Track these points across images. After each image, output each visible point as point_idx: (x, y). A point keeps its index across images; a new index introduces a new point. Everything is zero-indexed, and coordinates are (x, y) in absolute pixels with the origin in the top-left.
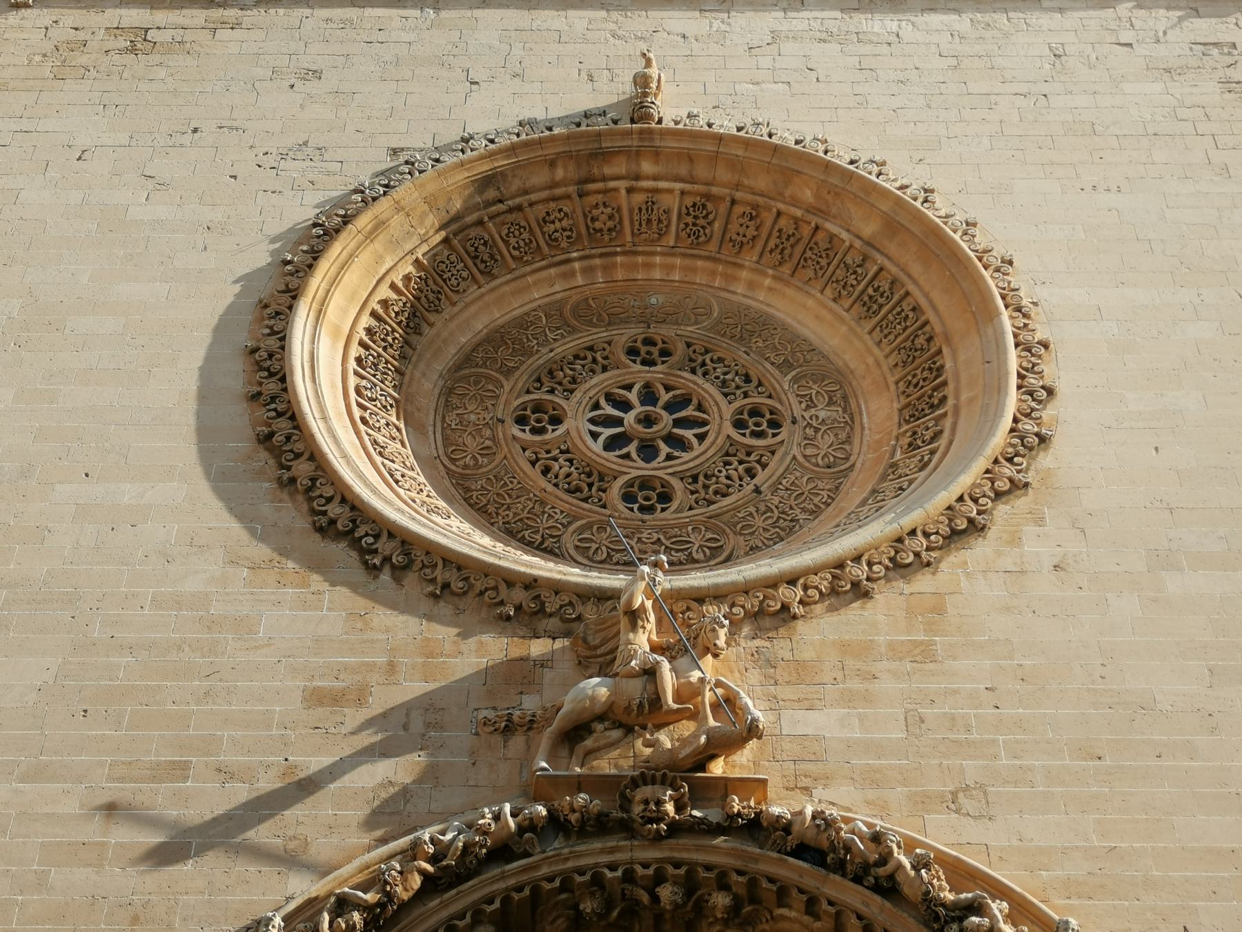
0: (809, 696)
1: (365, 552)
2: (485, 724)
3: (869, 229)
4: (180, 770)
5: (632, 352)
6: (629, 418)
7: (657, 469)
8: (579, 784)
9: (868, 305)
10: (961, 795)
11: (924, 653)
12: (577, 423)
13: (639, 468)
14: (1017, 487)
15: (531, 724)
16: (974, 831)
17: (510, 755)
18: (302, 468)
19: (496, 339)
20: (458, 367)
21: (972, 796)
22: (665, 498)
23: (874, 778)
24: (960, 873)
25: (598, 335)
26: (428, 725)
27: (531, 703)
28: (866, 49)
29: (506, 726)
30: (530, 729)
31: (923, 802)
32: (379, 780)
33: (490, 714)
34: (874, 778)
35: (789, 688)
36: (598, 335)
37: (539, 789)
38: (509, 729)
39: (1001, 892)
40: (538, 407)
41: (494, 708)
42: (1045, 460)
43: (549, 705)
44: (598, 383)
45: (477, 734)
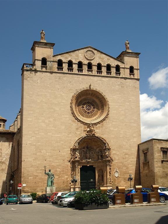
1: (78, 121)
3: (101, 97)
4: (71, 133)
5: (87, 103)
6: (87, 107)
7: (89, 111)
8: (88, 135)
9: (100, 101)
11: (102, 127)
12: (85, 108)
13: (88, 111)
14: (107, 117)
16: (104, 136)
18: (74, 115)
19: (80, 101)
20: (79, 103)
22: (89, 113)
23: (99, 133)
24: (103, 139)
25: (86, 101)
28: (102, 82)
31: (101, 135)
34: (99, 133)
36: (86, 101)
37: (86, 135)
38: (85, 131)
39: (104, 139)
40: (83, 107)
42: (108, 115)
44: (85, 106)
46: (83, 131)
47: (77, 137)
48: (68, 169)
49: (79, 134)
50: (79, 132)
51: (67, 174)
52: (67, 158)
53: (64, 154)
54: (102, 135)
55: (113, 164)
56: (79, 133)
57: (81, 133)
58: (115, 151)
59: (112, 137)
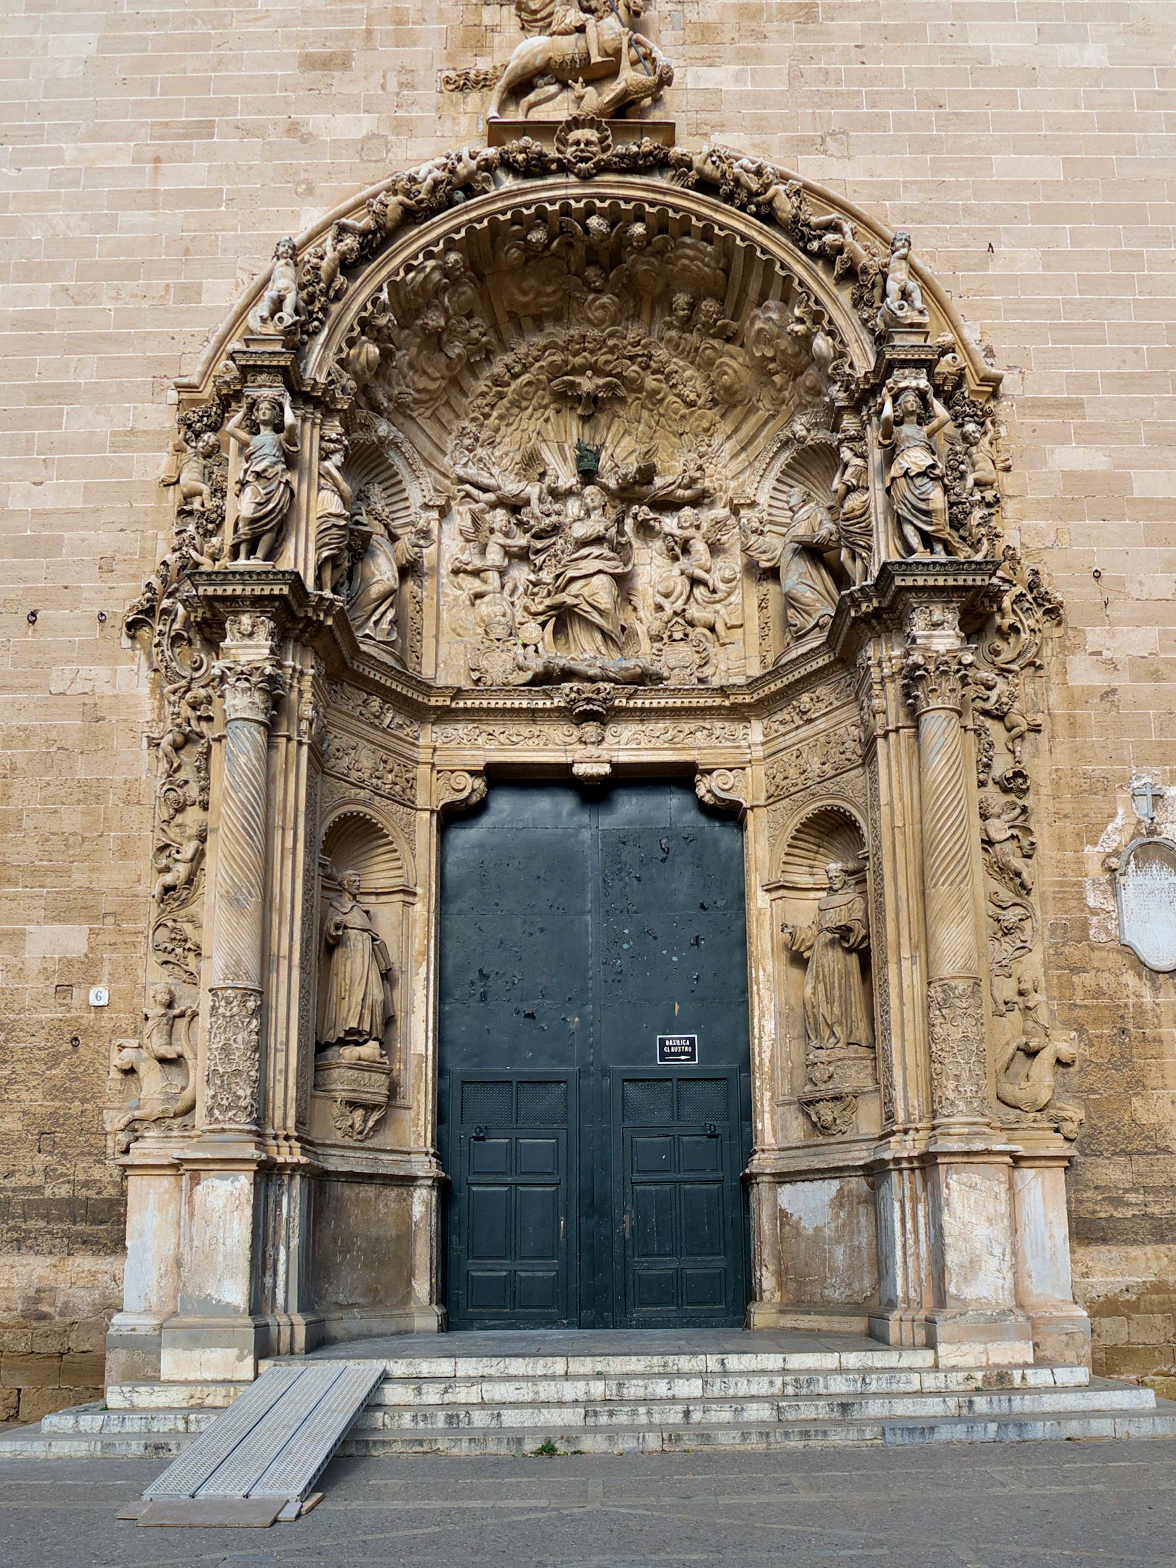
0: (711, 54)
2: (448, 82)
10: (828, 138)
15: (483, 83)
17: (469, 110)
21: (836, 140)
26: (401, 85)
27: (483, 65)
29: (465, 84)
30: (484, 86)
32: (364, 132)
33: (452, 74)
34: (759, 126)
35: (694, 47)
38: (464, 84)
41: (454, 69)
43: (498, 65)
45: (441, 92)
46: (429, 94)
47: (310, 191)
48: (93, 793)
49: (362, 146)
50: (348, 104)
51: (80, 878)
52: (106, 567)
53: (47, 500)
54: (819, 144)
55: (1073, 698)
56: (366, 123)
57: (403, 127)
58: (1089, 436)
59: (1020, 188)
